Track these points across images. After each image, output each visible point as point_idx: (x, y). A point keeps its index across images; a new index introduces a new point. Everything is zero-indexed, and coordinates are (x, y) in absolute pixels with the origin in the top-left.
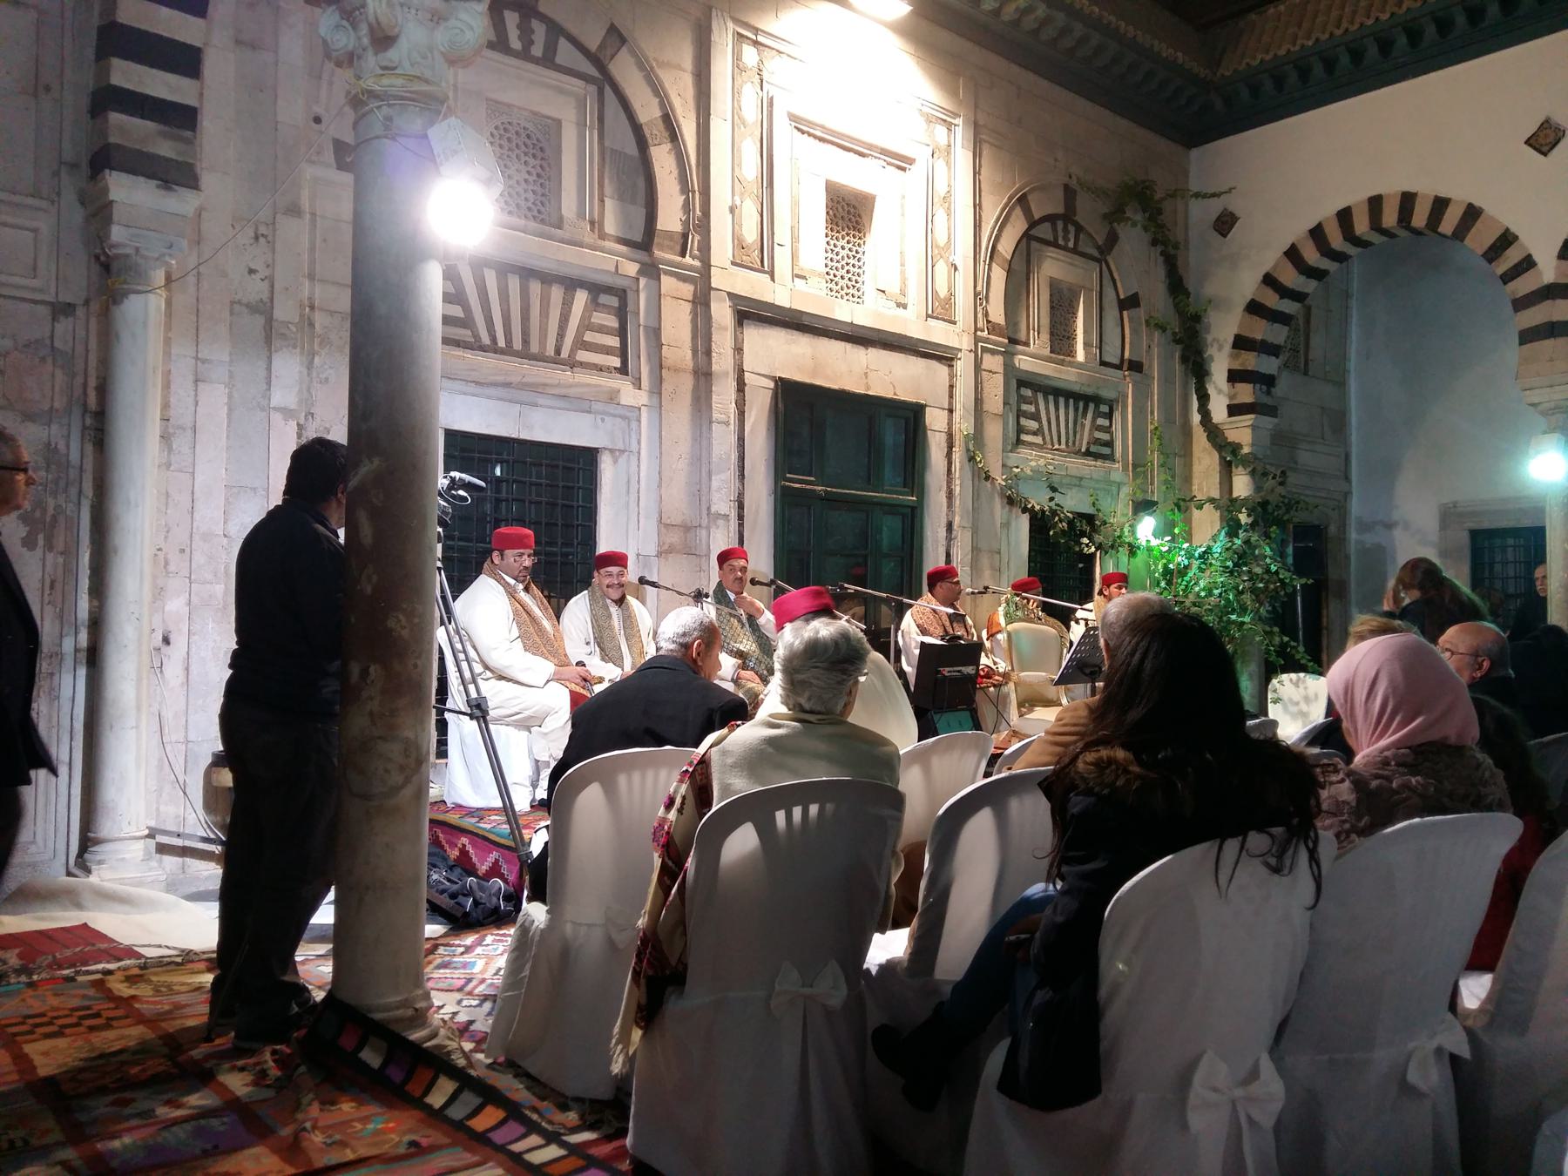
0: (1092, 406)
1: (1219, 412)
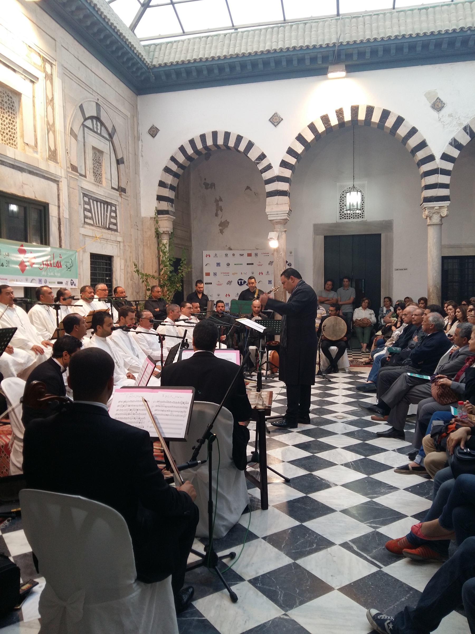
0: (109, 207)
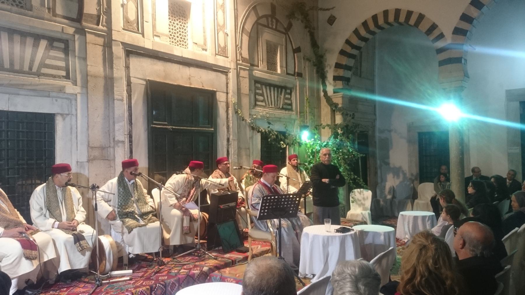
0: (284, 90)
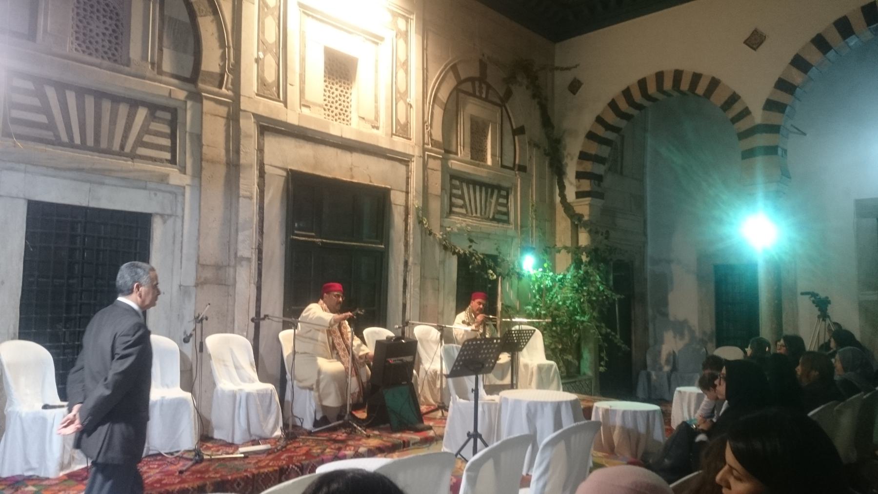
0: (496, 192)
1: (571, 196)
